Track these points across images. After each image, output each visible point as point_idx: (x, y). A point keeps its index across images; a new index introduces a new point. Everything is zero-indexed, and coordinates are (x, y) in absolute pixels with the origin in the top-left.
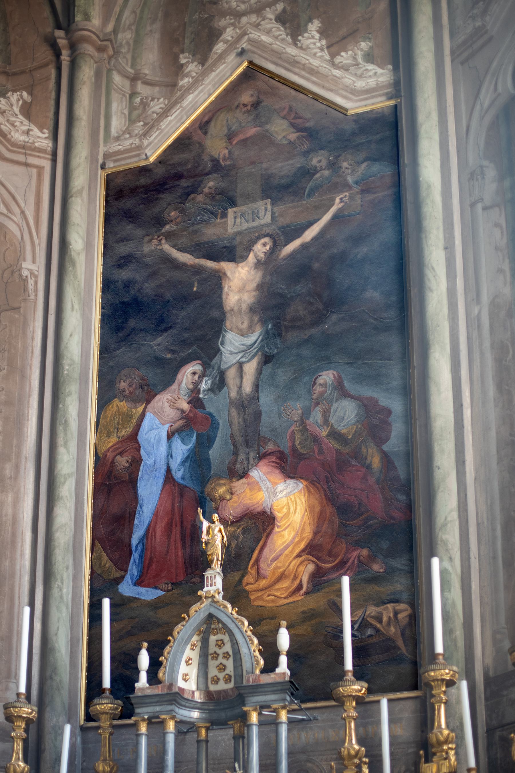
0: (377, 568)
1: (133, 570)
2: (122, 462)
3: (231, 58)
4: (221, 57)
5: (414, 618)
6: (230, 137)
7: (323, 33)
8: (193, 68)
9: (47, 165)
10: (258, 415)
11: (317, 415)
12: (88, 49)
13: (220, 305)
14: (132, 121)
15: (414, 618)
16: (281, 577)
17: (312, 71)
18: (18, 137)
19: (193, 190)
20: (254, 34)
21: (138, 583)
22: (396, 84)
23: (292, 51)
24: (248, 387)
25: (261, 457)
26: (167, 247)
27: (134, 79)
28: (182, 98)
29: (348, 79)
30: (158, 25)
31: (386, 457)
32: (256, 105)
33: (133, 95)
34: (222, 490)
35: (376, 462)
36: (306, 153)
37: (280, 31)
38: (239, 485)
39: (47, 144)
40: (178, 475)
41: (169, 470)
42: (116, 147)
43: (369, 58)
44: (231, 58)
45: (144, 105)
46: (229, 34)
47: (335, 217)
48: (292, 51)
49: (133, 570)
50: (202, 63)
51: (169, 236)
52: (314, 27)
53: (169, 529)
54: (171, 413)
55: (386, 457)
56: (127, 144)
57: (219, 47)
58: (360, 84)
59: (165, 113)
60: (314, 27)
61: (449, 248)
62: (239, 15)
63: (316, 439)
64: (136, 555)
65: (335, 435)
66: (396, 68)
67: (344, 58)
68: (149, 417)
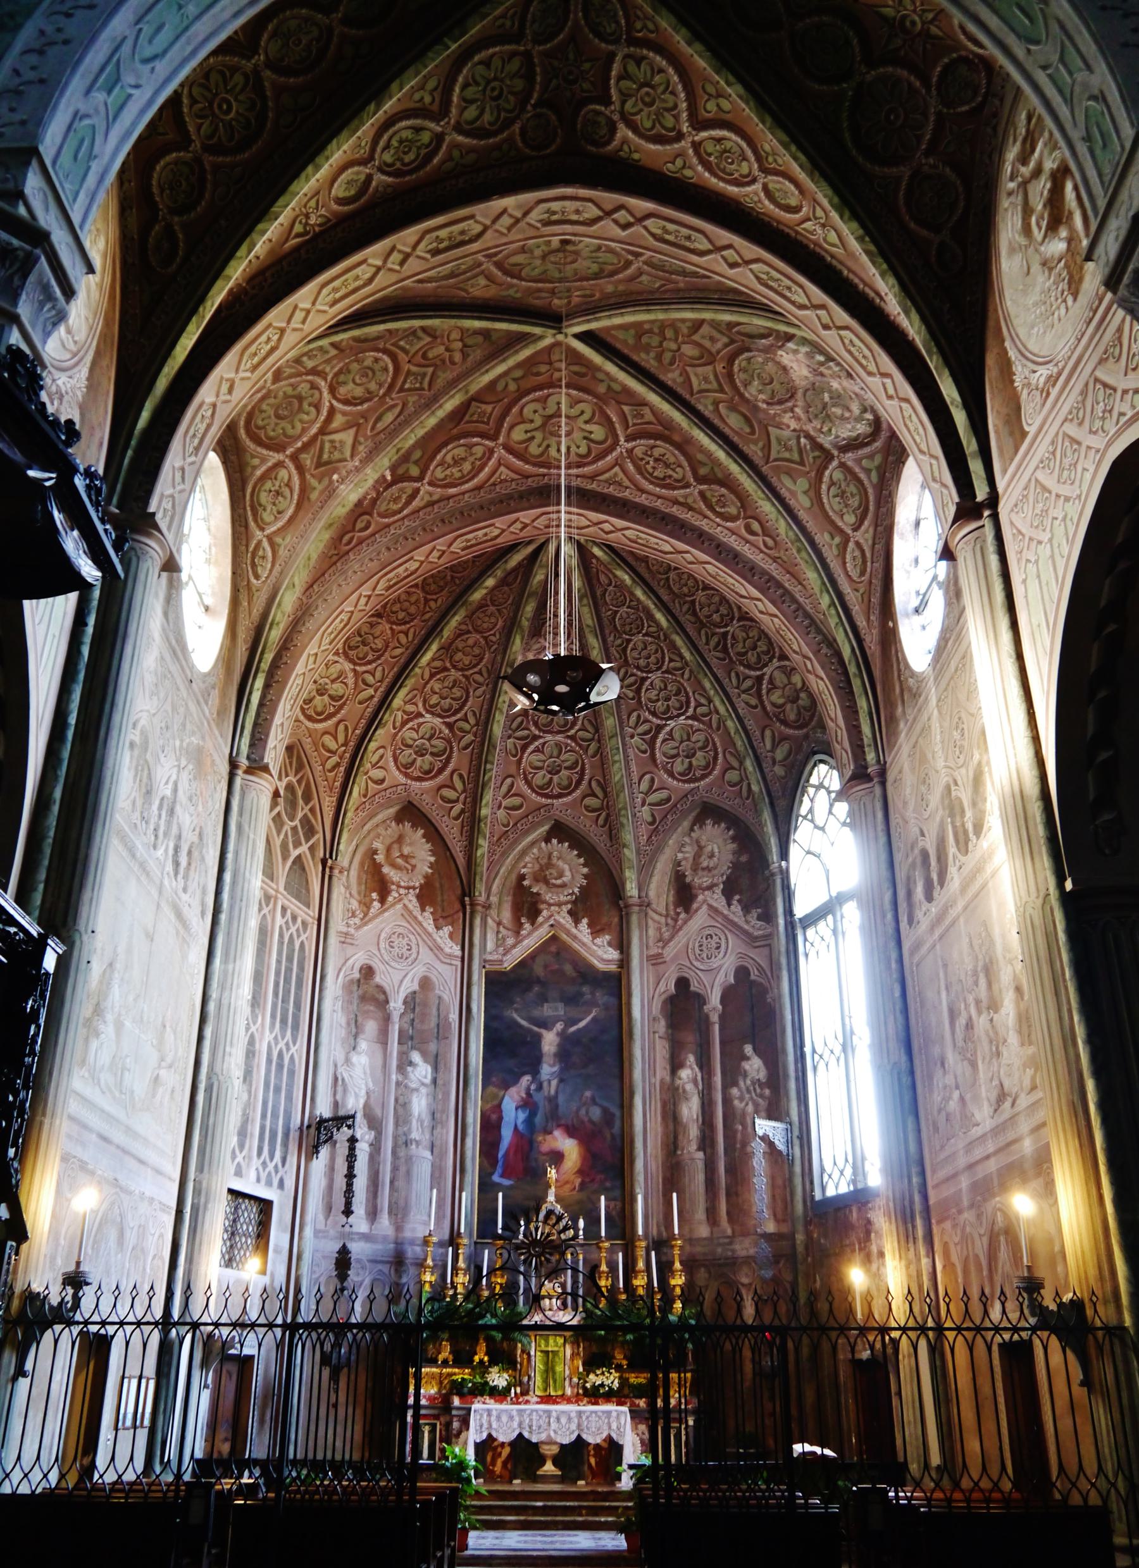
0: (608, 1184)
1: (499, 1170)
2: (494, 1117)
3: (546, 926)
4: (541, 924)
5: (623, 1209)
6: (546, 966)
7: (590, 925)
8: (527, 926)
9: (459, 964)
10: (557, 1106)
11: (583, 1112)
12: (479, 908)
13: (540, 1050)
14: (498, 946)
15: (623, 1209)
16: (567, 1182)
17: (584, 944)
18: (447, 950)
19: (528, 989)
20: (557, 917)
21: (502, 1176)
22: (621, 961)
23: (574, 931)
24: (553, 1092)
25: (559, 1126)
26: (515, 1016)
27: (499, 924)
28: (521, 941)
29: (600, 952)
30: (510, 898)
31: (612, 1135)
32: (558, 954)
33: (498, 932)
34: (540, 1138)
35: (608, 1136)
36: (582, 984)
37: (569, 919)
38: (548, 1137)
39: (459, 953)
40: (521, 1127)
41: (516, 1126)
42: (489, 957)
43: (610, 944)
44: (546, 926)
45: (504, 939)
46: (545, 913)
47: (594, 1020)
48: (574, 931)
49: (499, 1170)
50: (533, 924)
51: (516, 1010)
52: (585, 921)
53: (516, 1152)
54: (517, 1097)
55: (612, 1135)
56: (495, 957)
57: (540, 919)
58: (605, 956)
59: (514, 946)
60: (585, 921)
61: (643, 1050)
62: (550, 905)
63: (583, 1122)
64: (500, 1163)
65: (591, 1121)
66: (622, 953)
67: (598, 941)
68: (507, 1100)
